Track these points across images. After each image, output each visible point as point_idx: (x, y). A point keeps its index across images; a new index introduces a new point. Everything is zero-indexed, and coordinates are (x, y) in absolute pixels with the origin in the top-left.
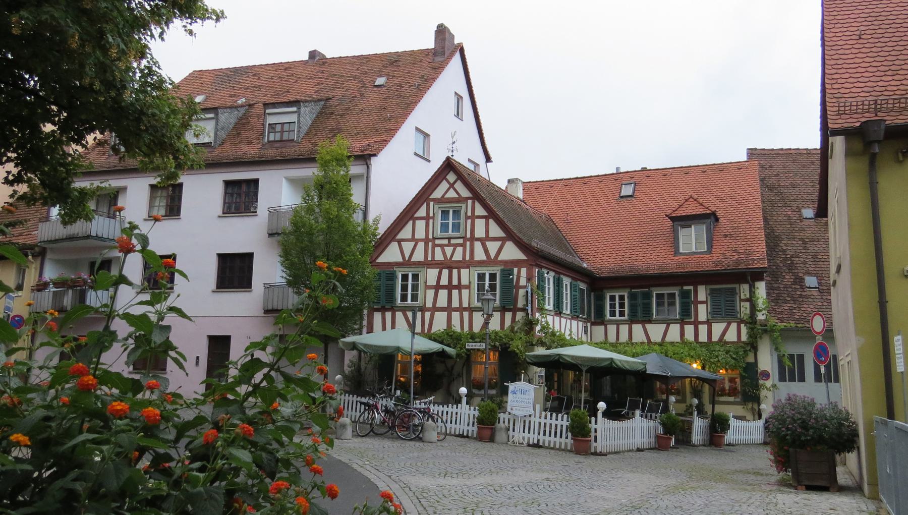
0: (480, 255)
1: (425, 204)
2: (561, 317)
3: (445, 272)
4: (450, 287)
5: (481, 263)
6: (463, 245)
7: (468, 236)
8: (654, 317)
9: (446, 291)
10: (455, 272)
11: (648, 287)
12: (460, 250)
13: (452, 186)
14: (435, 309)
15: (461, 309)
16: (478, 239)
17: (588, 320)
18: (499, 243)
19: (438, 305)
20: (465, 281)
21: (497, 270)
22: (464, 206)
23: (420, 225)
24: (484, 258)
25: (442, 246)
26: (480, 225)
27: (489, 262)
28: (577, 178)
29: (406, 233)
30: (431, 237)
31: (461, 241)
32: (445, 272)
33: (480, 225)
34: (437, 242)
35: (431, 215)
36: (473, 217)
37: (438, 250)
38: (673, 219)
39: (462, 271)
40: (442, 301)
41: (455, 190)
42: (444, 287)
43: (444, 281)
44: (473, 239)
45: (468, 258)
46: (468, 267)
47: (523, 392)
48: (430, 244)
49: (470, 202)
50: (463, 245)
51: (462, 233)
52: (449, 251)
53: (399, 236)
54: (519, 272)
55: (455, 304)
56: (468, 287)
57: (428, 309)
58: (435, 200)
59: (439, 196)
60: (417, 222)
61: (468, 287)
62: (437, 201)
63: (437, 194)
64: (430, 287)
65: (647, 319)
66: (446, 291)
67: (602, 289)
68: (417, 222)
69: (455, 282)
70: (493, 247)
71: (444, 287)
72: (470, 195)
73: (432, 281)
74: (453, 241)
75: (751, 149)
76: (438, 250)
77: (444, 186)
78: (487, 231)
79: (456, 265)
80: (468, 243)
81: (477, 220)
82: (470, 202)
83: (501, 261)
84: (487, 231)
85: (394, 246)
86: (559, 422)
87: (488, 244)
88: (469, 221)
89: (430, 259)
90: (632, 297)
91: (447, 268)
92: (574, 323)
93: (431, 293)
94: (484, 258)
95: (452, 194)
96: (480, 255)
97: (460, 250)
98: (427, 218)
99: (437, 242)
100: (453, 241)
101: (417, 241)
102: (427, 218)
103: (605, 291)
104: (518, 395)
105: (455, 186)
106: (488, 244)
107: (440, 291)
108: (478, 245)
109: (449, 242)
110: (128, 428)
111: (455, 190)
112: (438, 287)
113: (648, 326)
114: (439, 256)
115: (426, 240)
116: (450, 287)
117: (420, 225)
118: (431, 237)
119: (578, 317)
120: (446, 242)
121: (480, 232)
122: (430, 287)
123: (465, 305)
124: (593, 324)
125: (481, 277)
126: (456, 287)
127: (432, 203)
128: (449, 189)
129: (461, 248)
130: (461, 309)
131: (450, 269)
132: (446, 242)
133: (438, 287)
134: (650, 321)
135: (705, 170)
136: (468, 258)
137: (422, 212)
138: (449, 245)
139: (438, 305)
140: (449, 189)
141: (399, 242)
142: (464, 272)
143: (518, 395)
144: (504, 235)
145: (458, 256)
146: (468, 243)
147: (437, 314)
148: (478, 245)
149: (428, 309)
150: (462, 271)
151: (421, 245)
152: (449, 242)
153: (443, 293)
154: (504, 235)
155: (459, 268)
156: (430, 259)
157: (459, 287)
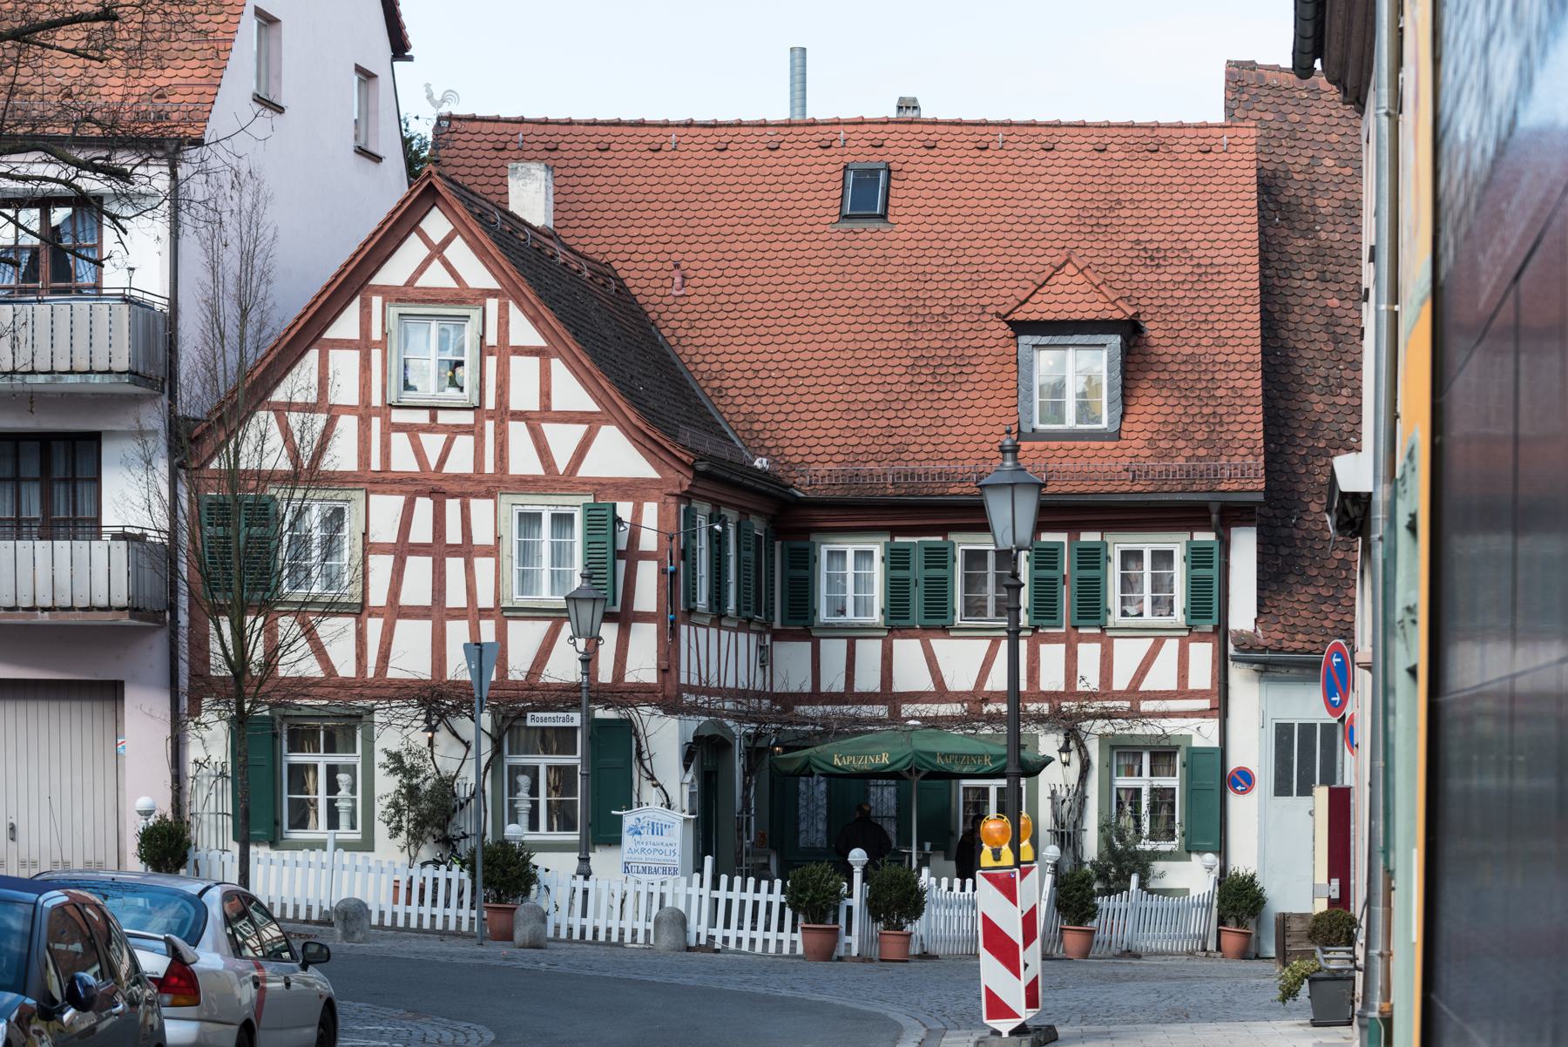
0: (524, 461)
1: (357, 302)
2: (720, 627)
3: (424, 506)
4: (438, 550)
5: (526, 484)
6: (475, 431)
7: (490, 404)
8: (958, 620)
9: (427, 562)
10: (453, 507)
11: (943, 530)
12: (464, 444)
13: (437, 251)
14: (396, 611)
15: (472, 613)
16: (520, 416)
17: (767, 627)
18: (582, 429)
19: (405, 599)
20: (482, 535)
21: (575, 505)
22: (476, 315)
23: (345, 364)
24: (538, 470)
25: (412, 430)
26: (525, 372)
27: (550, 482)
28: (690, 124)
29: (299, 383)
30: (376, 401)
31: (467, 418)
32: (424, 506)
33: (525, 372)
34: (398, 416)
35: (376, 335)
36: (505, 351)
37: (400, 441)
38: (1014, 325)
39: (475, 504)
40: (417, 590)
41: (447, 264)
42: (420, 549)
43: (421, 532)
44: (504, 414)
45: (489, 468)
46: (489, 494)
47: (657, 829)
48: (376, 422)
49: (492, 304)
50: (475, 431)
51: (469, 395)
52: (433, 444)
53: (279, 395)
54: (637, 513)
55: (456, 597)
56: (493, 551)
57: (376, 612)
58: (382, 290)
59: (400, 281)
60: (334, 354)
61: (493, 551)
62: (395, 295)
63: (394, 272)
64: (382, 549)
65: (937, 622)
66: (427, 562)
67: (807, 532)
68: (334, 354)
69: (454, 535)
70: (563, 440)
71: (420, 549)
72: (493, 284)
73: (385, 529)
74: (444, 418)
75: (1240, 65)
76: (400, 441)
77: (411, 252)
78: (546, 394)
79: (456, 488)
80: (490, 426)
81: (514, 360)
82: (492, 304)
83: (586, 482)
84: (546, 394)
85: (264, 419)
86: (763, 897)
87: (548, 429)
88: (491, 362)
89: (376, 465)
90: (897, 559)
91: (431, 493)
92: (742, 637)
93: (381, 566)
94: (538, 470)
95: (436, 277)
96: (524, 461)
97: (464, 444)
98: (364, 345)
99: (398, 416)
100: (444, 418)
101: (333, 413)
102: (364, 345)
103: (814, 538)
104: (647, 837)
105: (448, 253)
106: (548, 429)
107: (410, 560)
108: (518, 433)
109: (433, 418)
110: (110, 892)
111: (447, 264)
112: (402, 550)
113: (939, 645)
114: (403, 460)
115: (364, 412)
116: (438, 550)
117: (345, 364)
118: (376, 401)
119: (750, 620)
120: (422, 417)
121: (524, 396)
122: (382, 549)
123: (485, 600)
124: (778, 636)
125: (529, 520)
126: (455, 550)
127: (377, 301)
128: (427, 262)
129: (470, 439)
130: (472, 613)
131: (438, 495)
132: (422, 417)
133: (402, 550)
134: (945, 631)
135: (1103, 139)
136: (489, 468)
137: (346, 325)
138: (433, 427)
139: (405, 599)
140: (427, 262)
141: (281, 410)
142: (481, 509)
143: (647, 837)
144: (592, 406)
145: (461, 460)
146: (490, 426)
147: (401, 625)
148: (518, 433)
149: (376, 612)
150: (475, 504)
151: (348, 426)
152: (433, 418)
153: (419, 569)
154: (592, 406)
155: (464, 497)
156: (376, 465)
157: (467, 550)
